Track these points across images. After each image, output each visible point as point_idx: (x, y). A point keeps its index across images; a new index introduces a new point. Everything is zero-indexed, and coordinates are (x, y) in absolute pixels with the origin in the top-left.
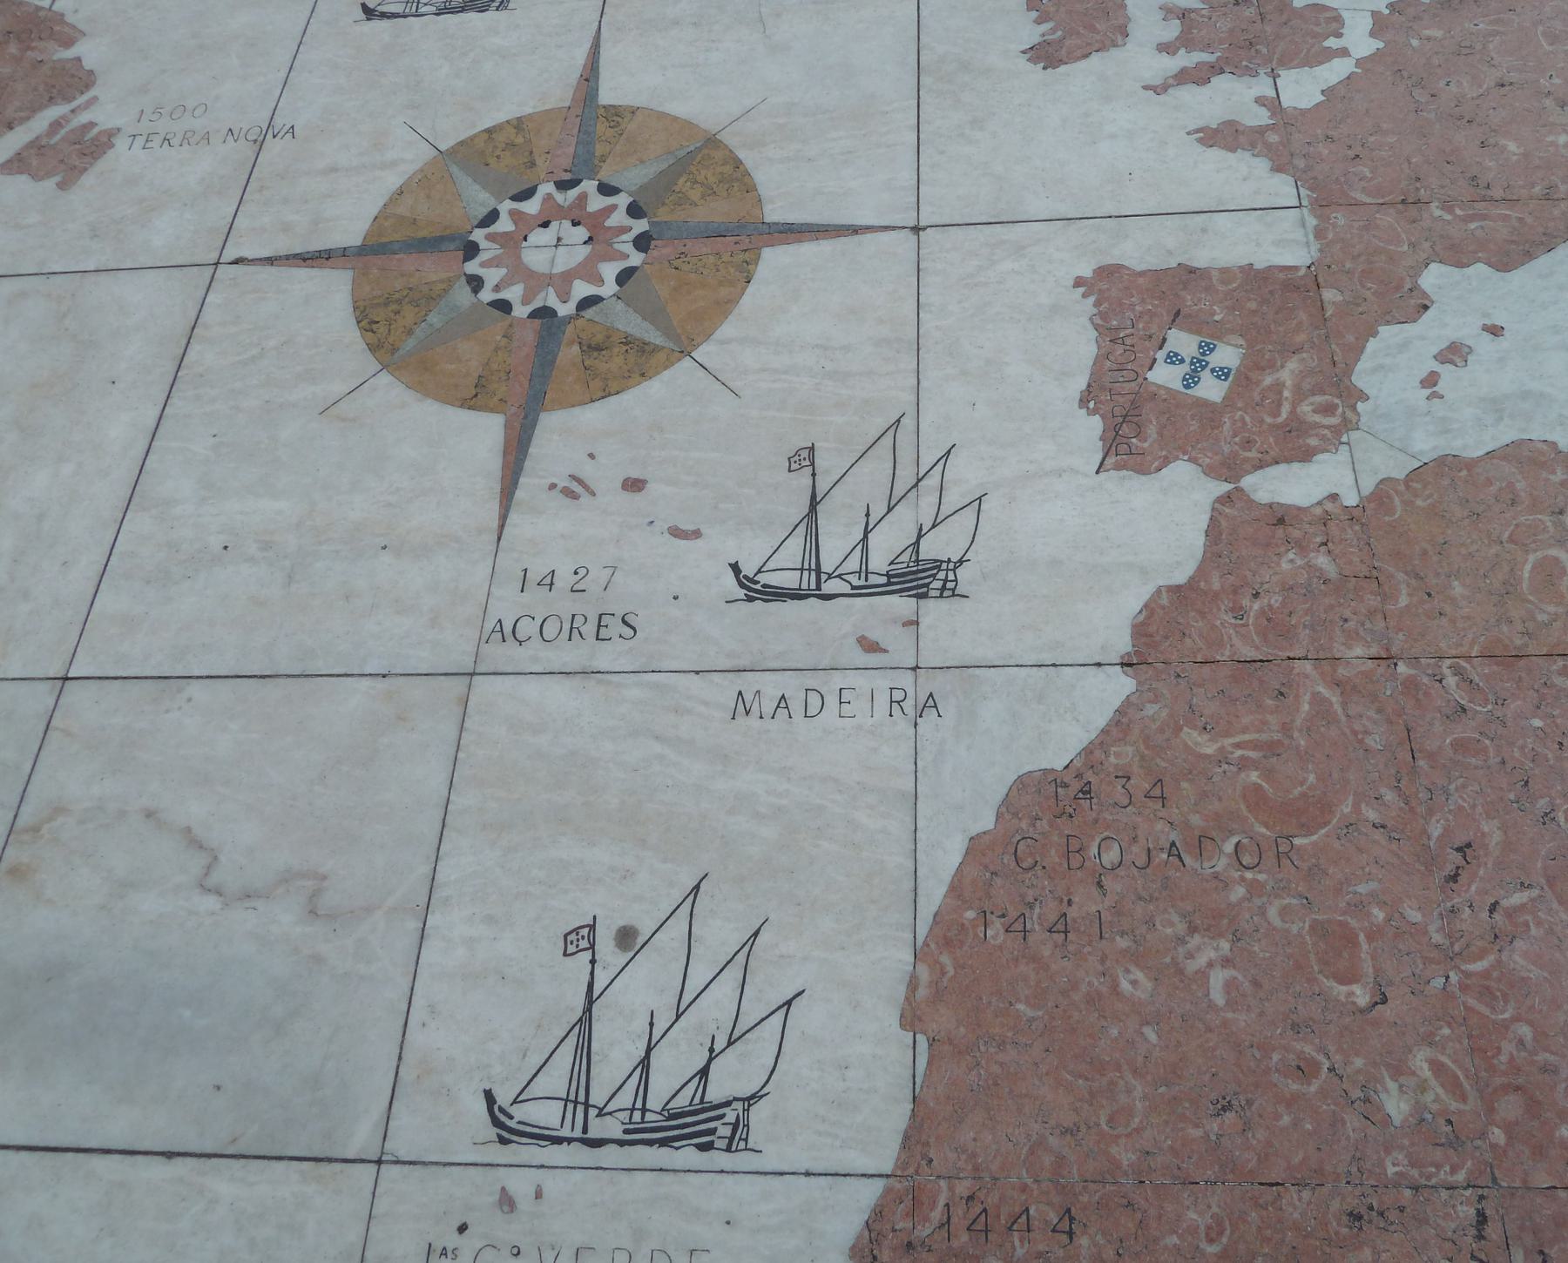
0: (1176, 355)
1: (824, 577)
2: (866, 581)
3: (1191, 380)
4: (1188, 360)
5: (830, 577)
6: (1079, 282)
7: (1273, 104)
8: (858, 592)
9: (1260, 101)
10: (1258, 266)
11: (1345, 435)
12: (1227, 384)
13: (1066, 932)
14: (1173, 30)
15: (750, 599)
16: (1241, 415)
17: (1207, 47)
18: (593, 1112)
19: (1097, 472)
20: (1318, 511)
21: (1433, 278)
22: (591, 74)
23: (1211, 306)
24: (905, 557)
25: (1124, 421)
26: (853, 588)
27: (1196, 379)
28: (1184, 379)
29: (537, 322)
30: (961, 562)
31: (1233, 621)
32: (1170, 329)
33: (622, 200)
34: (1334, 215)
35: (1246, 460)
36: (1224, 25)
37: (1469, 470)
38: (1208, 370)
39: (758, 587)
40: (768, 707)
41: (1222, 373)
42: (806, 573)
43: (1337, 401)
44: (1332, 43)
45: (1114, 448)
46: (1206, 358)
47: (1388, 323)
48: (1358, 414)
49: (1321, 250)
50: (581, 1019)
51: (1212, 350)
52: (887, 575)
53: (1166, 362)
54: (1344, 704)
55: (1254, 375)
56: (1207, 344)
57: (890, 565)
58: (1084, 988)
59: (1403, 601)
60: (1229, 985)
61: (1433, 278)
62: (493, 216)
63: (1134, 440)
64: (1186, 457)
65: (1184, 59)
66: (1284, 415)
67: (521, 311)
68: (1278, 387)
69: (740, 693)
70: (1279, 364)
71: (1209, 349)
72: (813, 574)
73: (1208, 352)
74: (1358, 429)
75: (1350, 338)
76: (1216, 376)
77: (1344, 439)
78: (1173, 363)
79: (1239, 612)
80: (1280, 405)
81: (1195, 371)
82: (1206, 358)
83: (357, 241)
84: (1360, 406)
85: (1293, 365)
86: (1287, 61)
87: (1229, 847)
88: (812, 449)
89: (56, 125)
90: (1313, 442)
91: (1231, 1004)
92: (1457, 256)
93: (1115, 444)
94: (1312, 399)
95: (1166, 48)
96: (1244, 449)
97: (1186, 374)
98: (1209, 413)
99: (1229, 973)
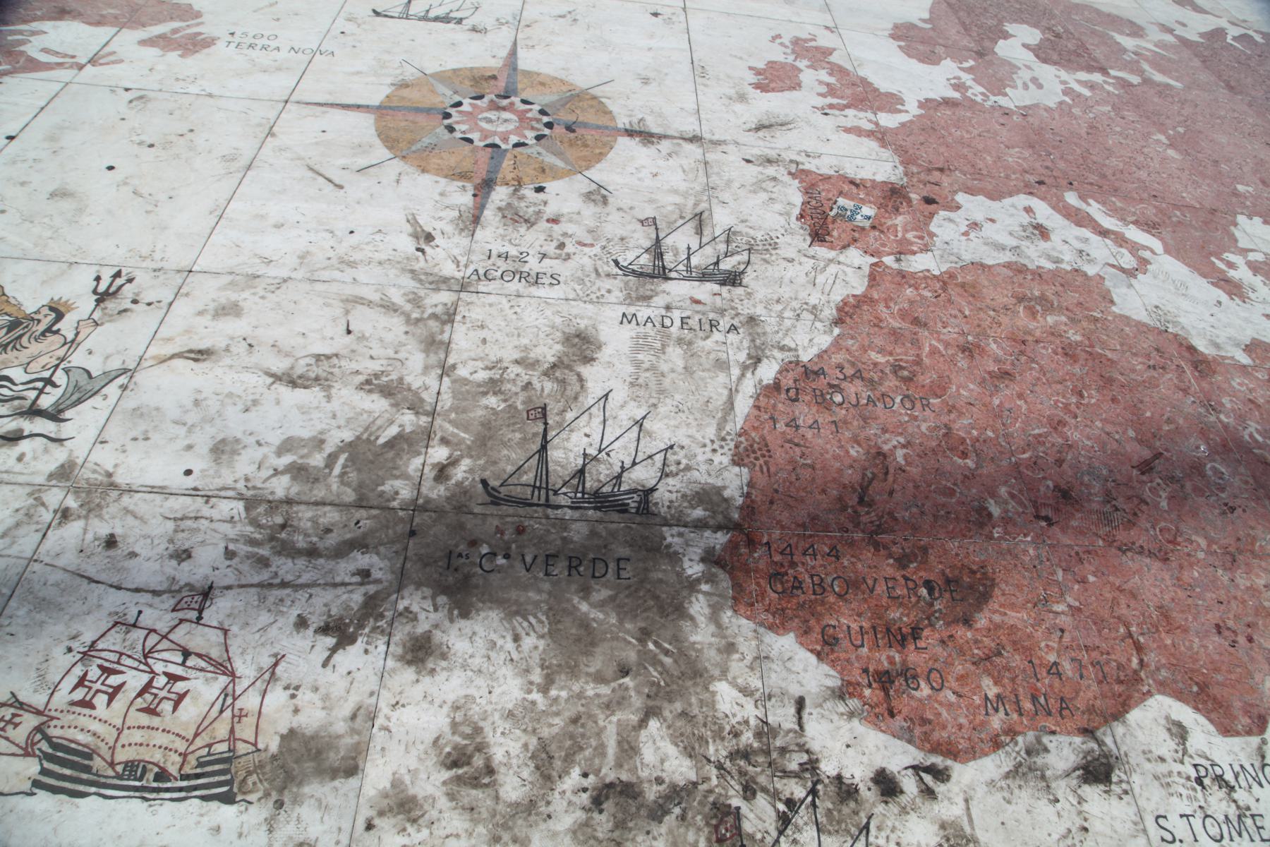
7: (877, 124)
9: (870, 121)
14: (824, 89)
17: (842, 98)
18: (551, 493)
21: (961, 198)
22: (513, 53)
29: (490, 150)
33: (536, 108)
36: (849, 92)
44: (899, 107)
50: (539, 451)
54: (946, 348)
58: (831, 453)
60: (905, 457)
61: (961, 198)
62: (459, 104)
65: (830, 100)
67: (479, 143)
79: (888, 307)
83: (377, 103)
86: (881, 109)
87: (898, 400)
88: (654, 218)
89: (175, 31)
91: (908, 464)
92: (971, 191)
95: (820, 95)
99: (905, 451)
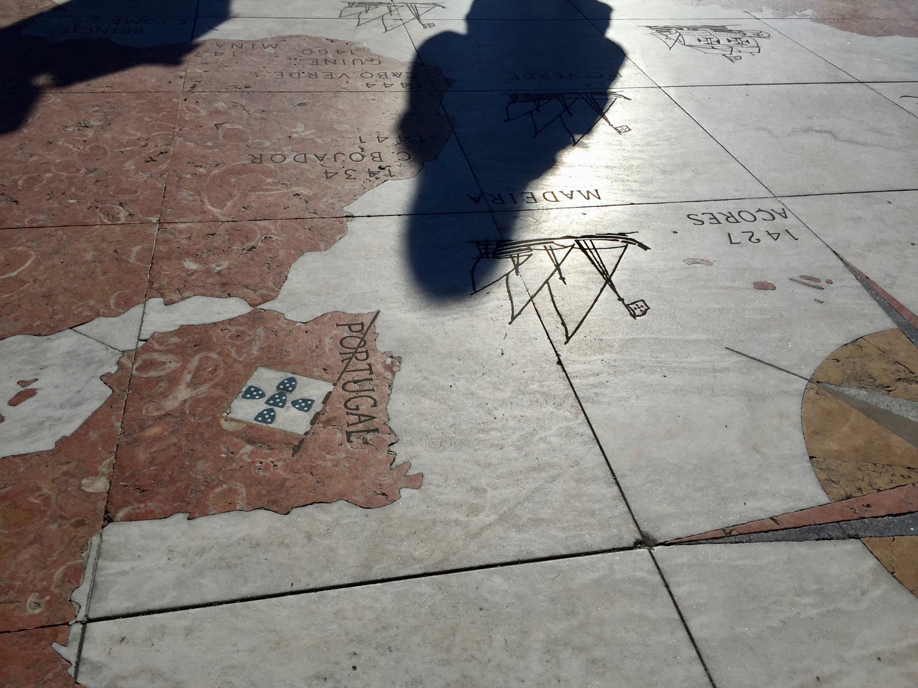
0: (301, 409)
1: (576, 246)
2: (545, 247)
3: (286, 387)
4: (289, 404)
5: (573, 247)
6: (416, 481)
8: (550, 241)
10: (180, 517)
11: (139, 346)
12: (249, 383)
13: (378, 137)
15: (623, 234)
16: (240, 356)
19: (378, 312)
20: (186, 294)
23: (253, 462)
24: (521, 259)
25: (356, 349)
26: (553, 242)
27: (281, 387)
28: (294, 387)
30: (479, 258)
31: (272, 236)
32: (306, 433)
34: (38, 611)
35: (242, 325)
37: (31, 326)
38: (269, 394)
39: (620, 240)
40: (576, 194)
41: (253, 393)
42: (591, 246)
43: (134, 372)
45: (365, 328)
46: (269, 407)
47: (39, 454)
48: (118, 363)
49: (84, 547)
51: (261, 414)
52: (531, 250)
53: (313, 401)
55: (218, 392)
56: (264, 420)
57: (532, 254)
59: (135, 249)
63: (346, 335)
64: (298, 324)
66: (195, 361)
68: (194, 384)
69: (599, 198)
70: (187, 406)
71: (267, 416)
72: (585, 247)
73: (265, 412)
74: (123, 352)
75: (94, 436)
76: (260, 390)
77: (141, 344)
78: (305, 401)
80: (198, 369)
81: (281, 395)
82: (269, 407)
84: (113, 369)
85: (171, 404)
90: (175, 340)
93: (365, 331)
94: (162, 373)
96: (242, 332)
97: (291, 391)
98: (272, 360)
